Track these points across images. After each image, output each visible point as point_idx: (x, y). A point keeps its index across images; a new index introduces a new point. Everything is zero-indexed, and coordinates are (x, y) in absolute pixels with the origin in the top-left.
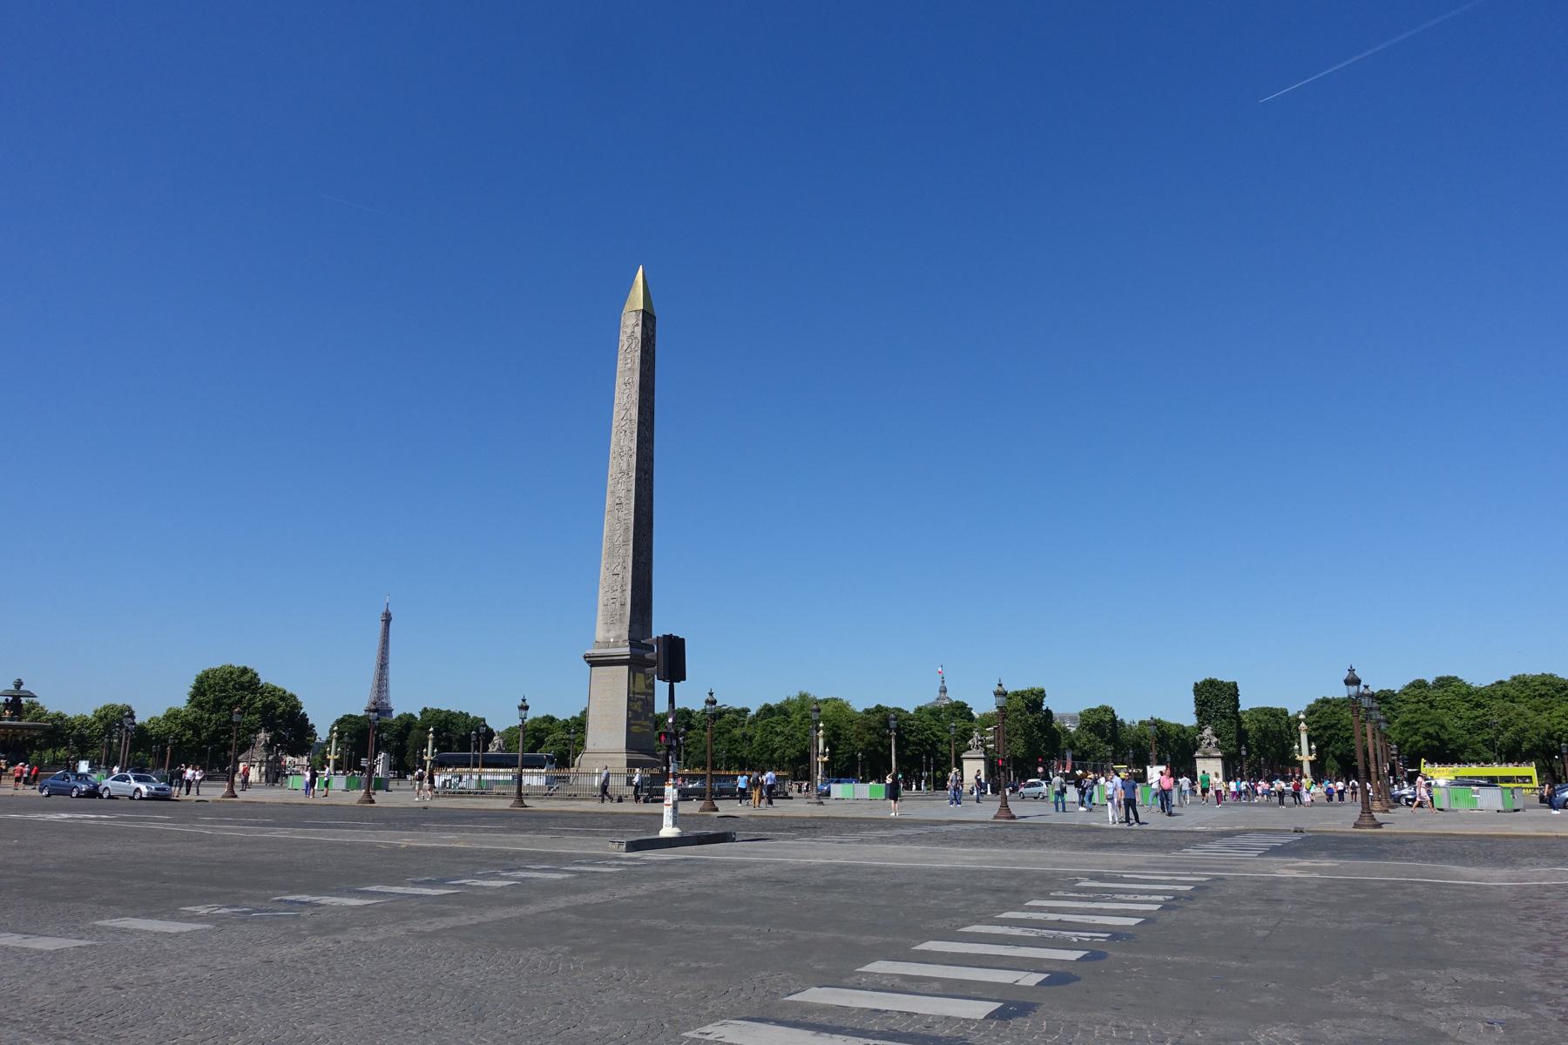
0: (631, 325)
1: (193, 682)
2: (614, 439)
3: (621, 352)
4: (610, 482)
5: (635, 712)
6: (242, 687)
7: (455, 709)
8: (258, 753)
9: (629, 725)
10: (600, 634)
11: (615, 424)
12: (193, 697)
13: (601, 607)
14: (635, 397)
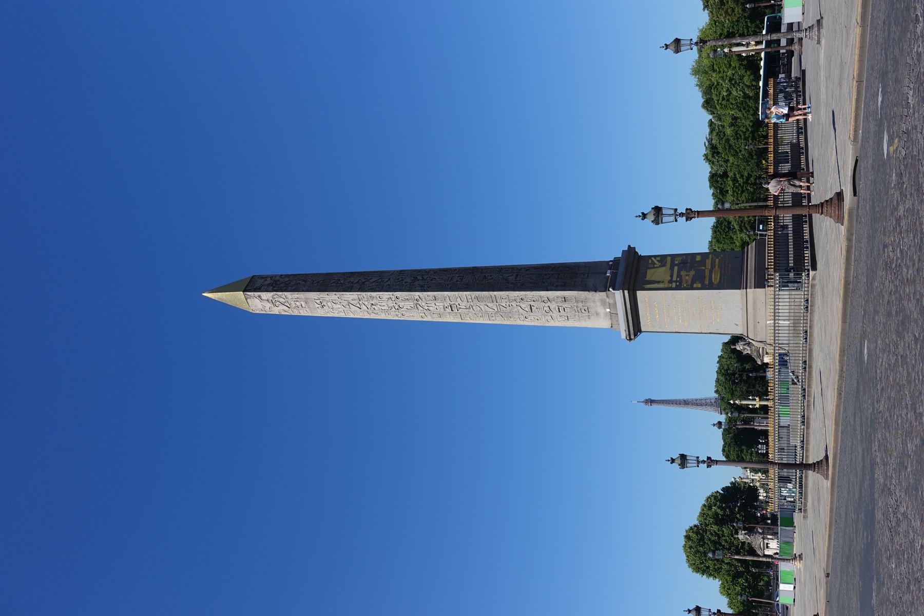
0: (260, 303)
1: (698, 575)
2: (383, 316)
3: (290, 312)
4: (429, 319)
5: (693, 282)
6: (702, 539)
7: (716, 367)
8: (756, 541)
9: (711, 287)
10: (603, 323)
11: (367, 316)
12: (710, 575)
13: (571, 324)
14: (333, 296)
